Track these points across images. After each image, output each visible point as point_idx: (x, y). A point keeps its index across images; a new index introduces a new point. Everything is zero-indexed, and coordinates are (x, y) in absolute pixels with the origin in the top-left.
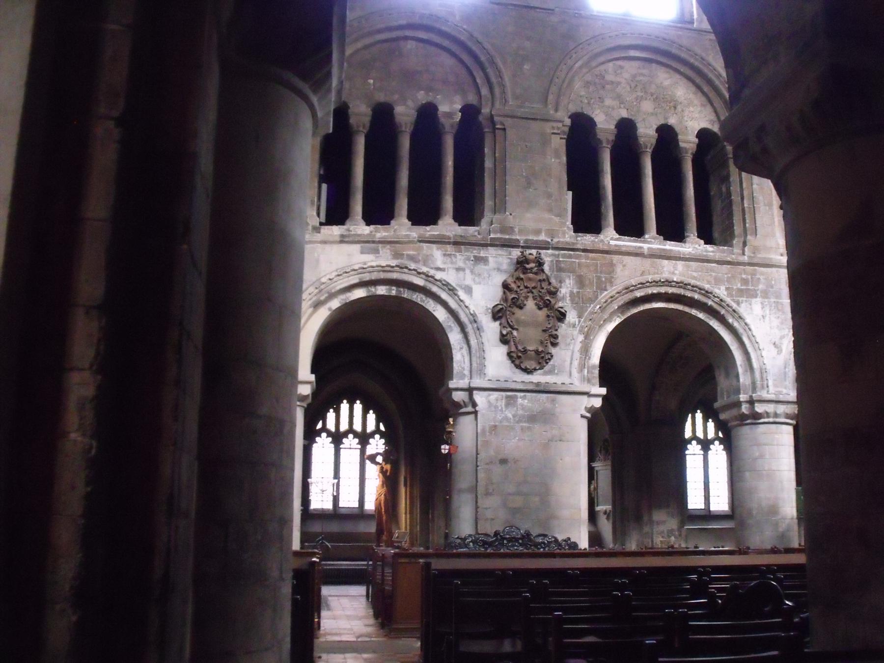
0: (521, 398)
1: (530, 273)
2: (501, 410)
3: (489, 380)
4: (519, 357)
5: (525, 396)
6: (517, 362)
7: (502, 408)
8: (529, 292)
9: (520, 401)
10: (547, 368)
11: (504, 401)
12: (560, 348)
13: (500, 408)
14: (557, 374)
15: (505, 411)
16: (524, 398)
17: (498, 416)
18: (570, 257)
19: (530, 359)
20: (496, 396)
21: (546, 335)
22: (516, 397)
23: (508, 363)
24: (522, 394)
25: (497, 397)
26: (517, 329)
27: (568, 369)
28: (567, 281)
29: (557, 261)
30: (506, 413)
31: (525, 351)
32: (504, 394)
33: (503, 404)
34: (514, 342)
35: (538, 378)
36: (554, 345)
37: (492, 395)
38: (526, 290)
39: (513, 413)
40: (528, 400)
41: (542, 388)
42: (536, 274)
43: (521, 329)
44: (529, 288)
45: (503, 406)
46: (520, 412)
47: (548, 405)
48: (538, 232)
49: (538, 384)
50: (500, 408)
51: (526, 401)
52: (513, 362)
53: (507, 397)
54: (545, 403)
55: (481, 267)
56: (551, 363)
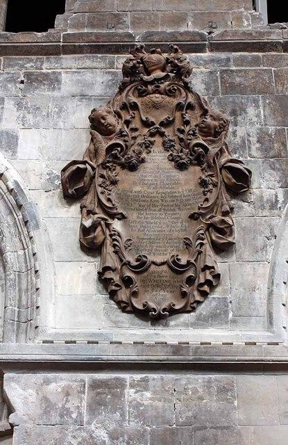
0: (132, 386)
1: (154, 92)
2: (79, 422)
3: (44, 342)
4: (128, 282)
5: (145, 380)
6: (123, 295)
7: (80, 414)
8: (152, 135)
9: (130, 393)
10: (204, 309)
11: (85, 397)
12: (240, 259)
13: (74, 416)
14: (234, 322)
15: (89, 423)
16: (143, 386)
17: (69, 438)
18: (256, 61)
19: (159, 285)
20: (63, 383)
21: (199, 227)
22: (121, 384)
23: (101, 300)
24: (138, 376)
25: (69, 387)
26: (122, 217)
27: (263, 310)
28: (251, 111)
29: (223, 72)
30: (93, 427)
31: (141, 266)
32: (87, 377)
33: (84, 403)
34: (114, 246)
35: (178, 332)
36: (223, 249)
37: (55, 380)
38: (146, 131)
39: (112, 427)
40: (154, 392)
41: (190, 358)
42: (170, 93)
43: (133, 216)
44: (153, 124)
45: (84, 410)
46: (132, 425)
47: (212, 403)
48: (180, 19)
49: (178, 348)
50: (74, 416)
51: (148, 394)
52: (113, 295)
53: (95, 385)
54: (201, 398)
55: (42, 95)
56: (217, 293)
